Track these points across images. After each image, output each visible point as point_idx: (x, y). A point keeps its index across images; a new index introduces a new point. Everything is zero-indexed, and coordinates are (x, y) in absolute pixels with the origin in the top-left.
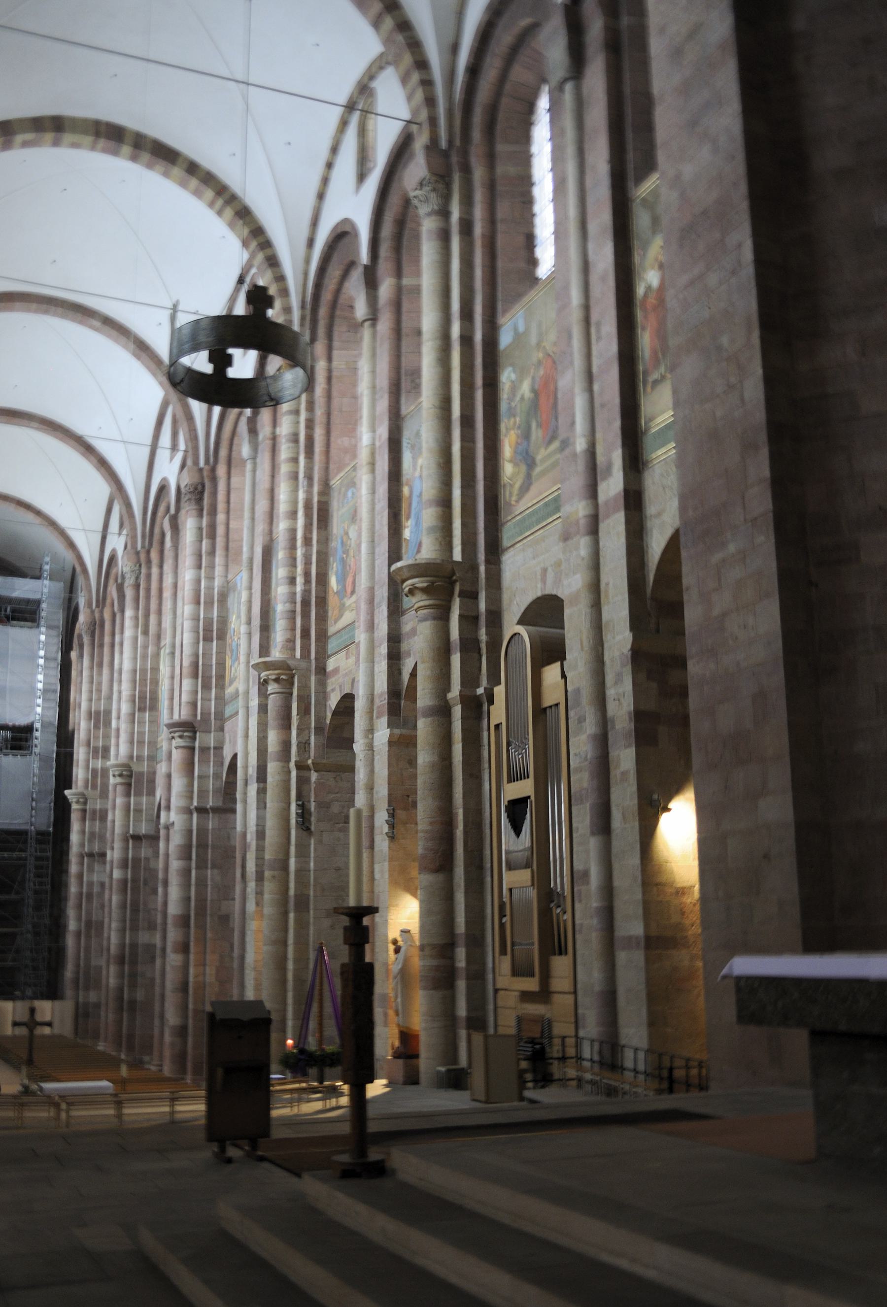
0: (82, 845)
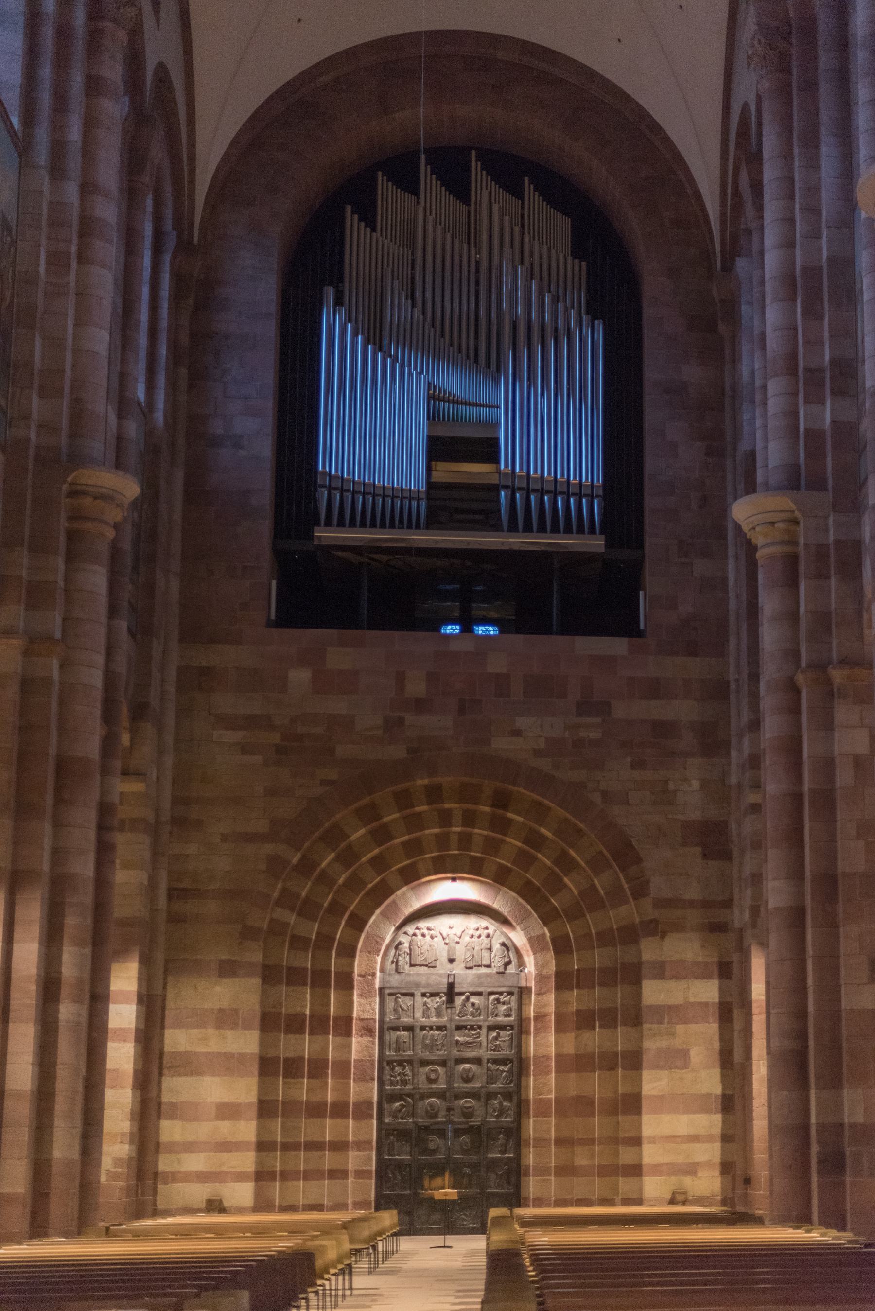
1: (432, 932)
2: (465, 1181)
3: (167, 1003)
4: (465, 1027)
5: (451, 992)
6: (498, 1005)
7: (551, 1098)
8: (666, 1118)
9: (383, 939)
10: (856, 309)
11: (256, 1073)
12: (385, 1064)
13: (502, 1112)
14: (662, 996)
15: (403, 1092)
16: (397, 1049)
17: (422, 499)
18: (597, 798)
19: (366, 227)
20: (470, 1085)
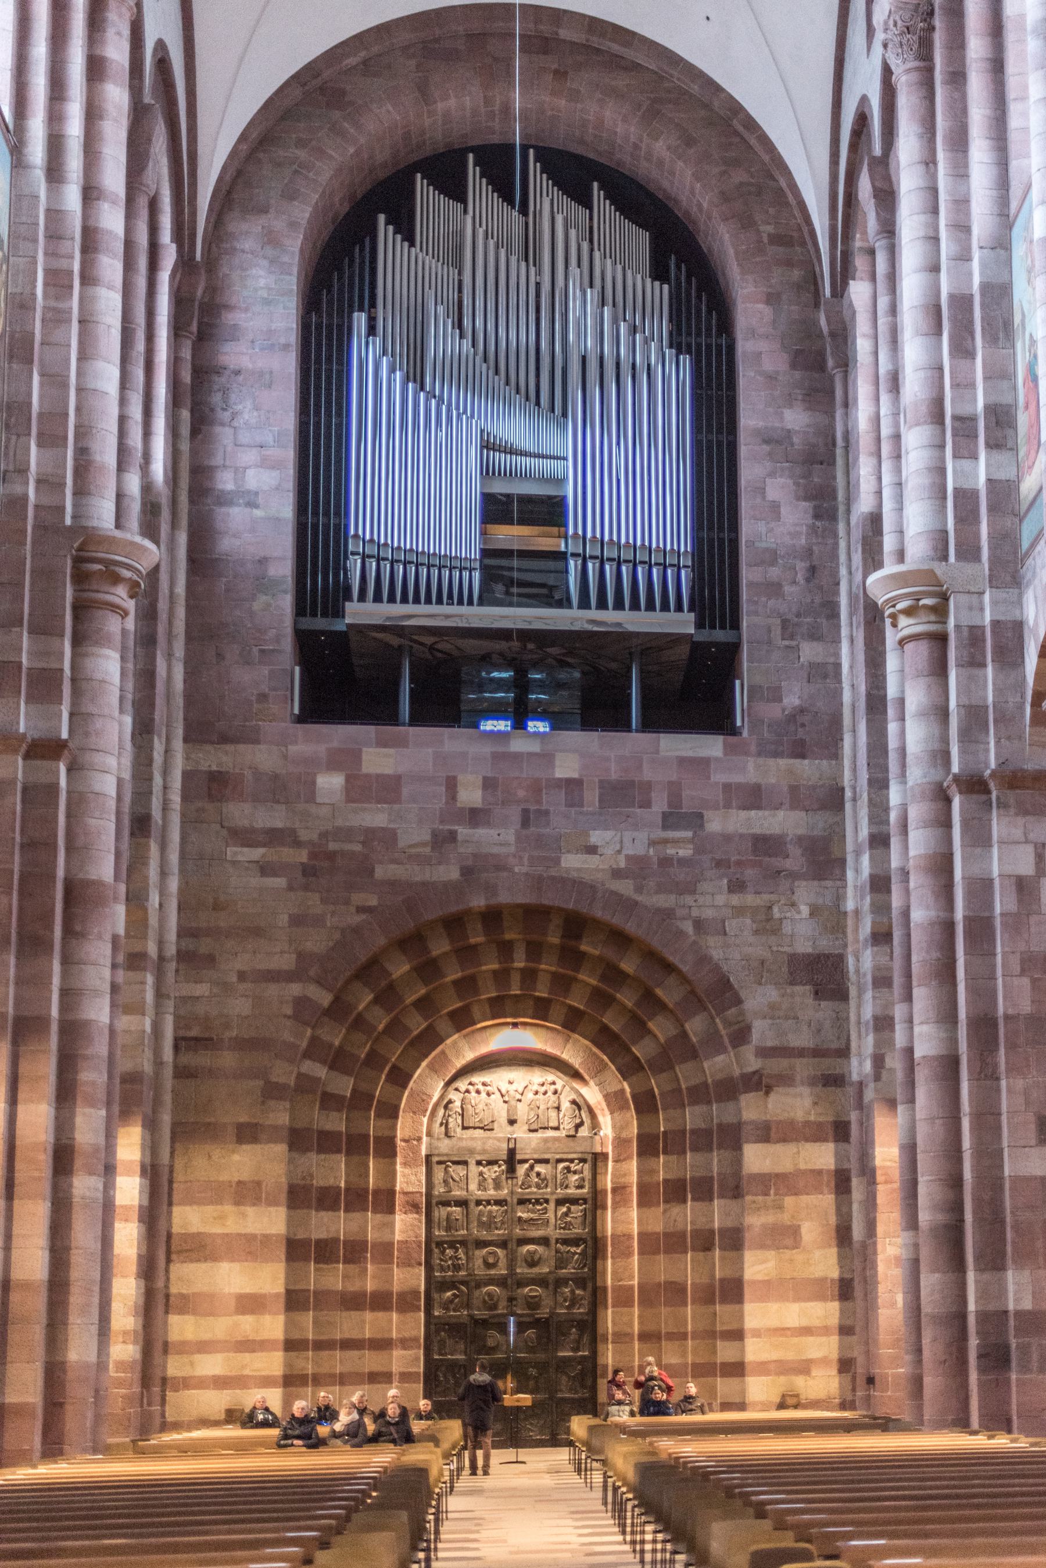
0: (943, 756)
1: (488, 1088)
2: (532, 1383)
3: (175, 1175)
4: (529, 1201)
5: (512, 1160)
6: (569, 1175)
7: (632, 1287)
8: (774, 1307)
9: (430, 1097)
10: (1013, 347)
11: (283, 1257)
12: (434, 1246)
13: (574, 1301)
14: (768, 1162)
15: (456, 1279)
16: (448, 1228)
17: (475, 569)
18: (688, 927)
19: (403, 240)
20: (536, 1270)
